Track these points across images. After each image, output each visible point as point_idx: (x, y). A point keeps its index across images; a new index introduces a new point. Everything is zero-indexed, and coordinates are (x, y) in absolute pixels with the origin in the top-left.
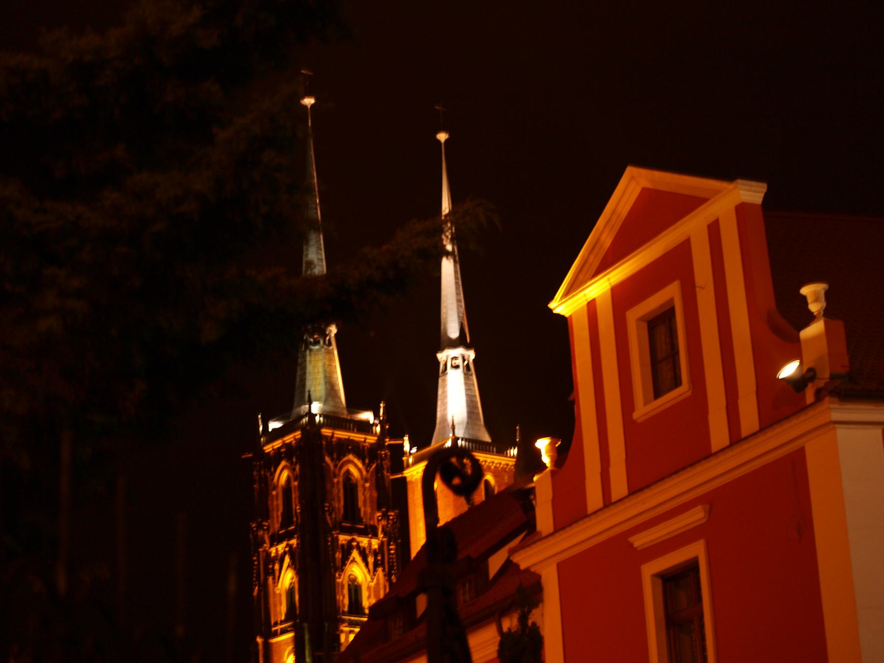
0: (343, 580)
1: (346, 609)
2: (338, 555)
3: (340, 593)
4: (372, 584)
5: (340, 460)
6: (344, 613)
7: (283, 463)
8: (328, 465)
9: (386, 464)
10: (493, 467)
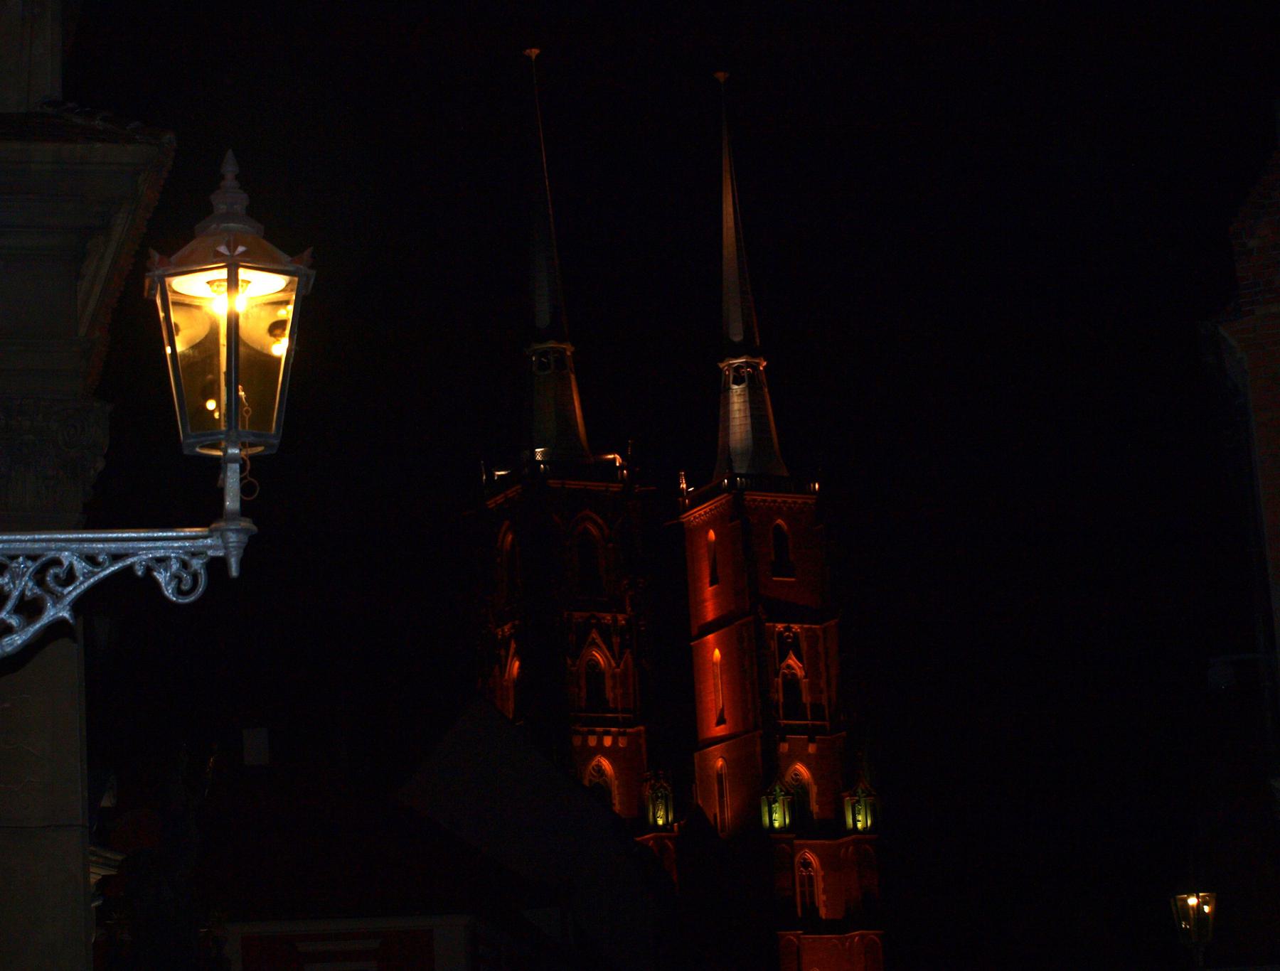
10: (785, 509)
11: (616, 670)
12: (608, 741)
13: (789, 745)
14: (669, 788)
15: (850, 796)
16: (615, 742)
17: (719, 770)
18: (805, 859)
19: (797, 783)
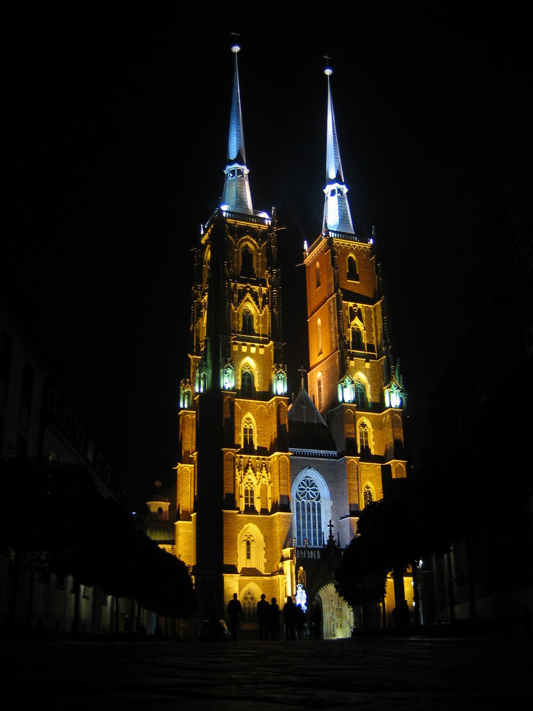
0: (238, 311)
1: (240, 330)
2: (236, 296)
3: (236, 320)
4: (261, 315)
5: (240, 238)
6: (238, 332)
7: (209, 246)
8: (231, 241)
9: (272, 241)
10: (354, 249)
11: (260, 315)
12: (253, 350)
13: (355, 363)
14: (285, 374)
15: (388, 388)
16: (257, 350)
17: (319, 378)
18: (363, 423)
19: (360, 383)
